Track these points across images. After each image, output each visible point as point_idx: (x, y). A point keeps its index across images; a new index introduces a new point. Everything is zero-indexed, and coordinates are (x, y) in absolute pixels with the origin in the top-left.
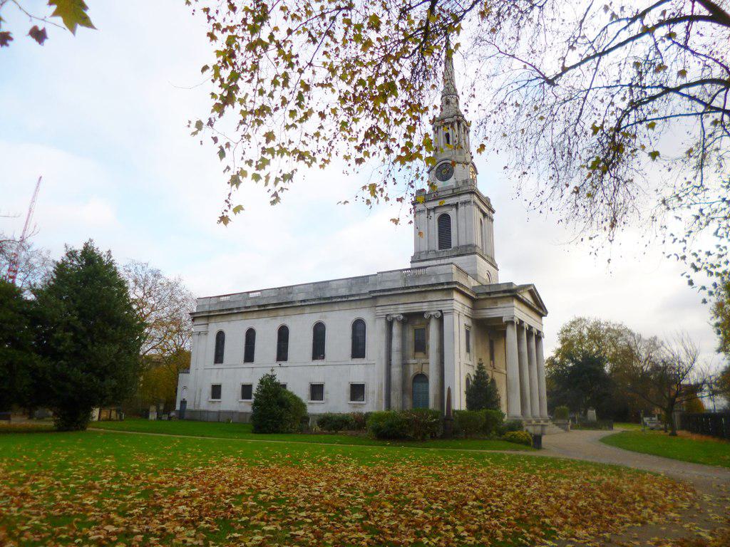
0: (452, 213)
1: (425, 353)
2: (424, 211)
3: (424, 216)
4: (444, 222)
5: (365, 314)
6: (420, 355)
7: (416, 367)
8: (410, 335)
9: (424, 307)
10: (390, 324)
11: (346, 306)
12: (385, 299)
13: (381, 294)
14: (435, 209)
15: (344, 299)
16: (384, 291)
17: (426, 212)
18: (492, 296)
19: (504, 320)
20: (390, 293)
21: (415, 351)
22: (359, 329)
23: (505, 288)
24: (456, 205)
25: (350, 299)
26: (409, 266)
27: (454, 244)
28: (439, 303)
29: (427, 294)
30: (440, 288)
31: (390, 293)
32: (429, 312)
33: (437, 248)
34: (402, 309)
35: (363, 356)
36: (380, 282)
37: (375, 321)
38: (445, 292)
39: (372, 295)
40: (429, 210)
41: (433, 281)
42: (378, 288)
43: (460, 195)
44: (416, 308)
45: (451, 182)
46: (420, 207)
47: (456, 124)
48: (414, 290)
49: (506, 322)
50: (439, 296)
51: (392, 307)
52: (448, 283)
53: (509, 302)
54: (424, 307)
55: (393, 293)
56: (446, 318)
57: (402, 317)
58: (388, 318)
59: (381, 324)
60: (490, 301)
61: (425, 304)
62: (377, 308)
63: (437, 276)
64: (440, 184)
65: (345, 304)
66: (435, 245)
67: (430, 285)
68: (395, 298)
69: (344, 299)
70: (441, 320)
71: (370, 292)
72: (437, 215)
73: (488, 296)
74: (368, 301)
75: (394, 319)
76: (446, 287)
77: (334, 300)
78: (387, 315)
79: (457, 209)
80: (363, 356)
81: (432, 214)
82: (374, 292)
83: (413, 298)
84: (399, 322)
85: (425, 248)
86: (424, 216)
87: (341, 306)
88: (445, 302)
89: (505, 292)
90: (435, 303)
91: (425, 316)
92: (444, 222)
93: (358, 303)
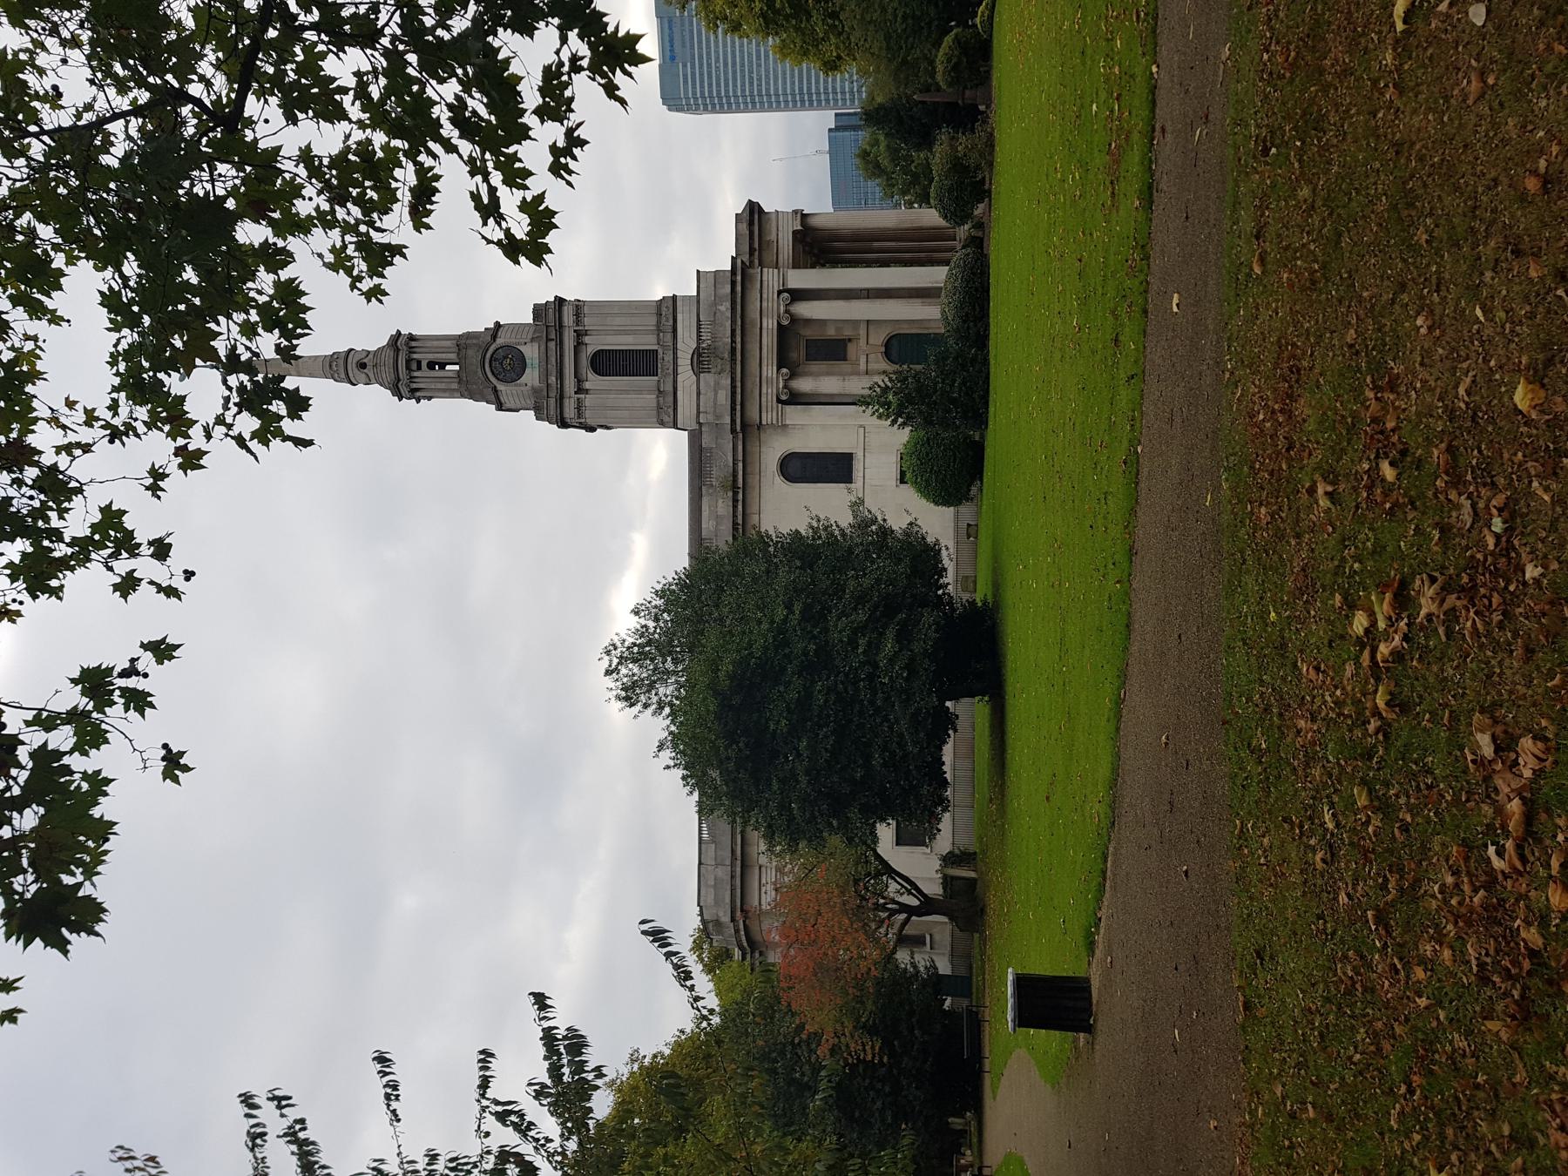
0: (593, 344)
1: (850, 340)
2: (578, 399)
3: (588, 400)
4: (607, 363)
5: (773, 451)
6: (851, 348)
7: (872, 357)
8: (815, 366)
9: (770, 326)
10: (795, 399)
11: (753, 495)
12: (748, 405)
13: (738, 407)
14: (579, 380)
15: (740, 496)
16: (733, 409)
17: (583, 396)
18: (756, 246)
19: (799, 228)
20: (739, 390)
21: (845, 359)
22: (802, 468)
23: (744, 226)
24: (579, 335)
25: (740, 483)
26: (683, 436)
27: (647, 342)
28: (765, 296)
29: (748, 321)
30: (739, 288)
31: (739, 390)
32: (779, 317)
33: (656, 378)
34: (770, 370)
35: (848, 458)
36: (718, 417)
37: (785, 426)
38: (748, 285)
39: (738, 428)
40: (580, 390)
41: (725, 307)
42: (728, 420)
43: (561, 326)
44: (769, 340)
45: (531, 352)
46: (570, 412)
47: (413, 344)
48: (738, 339)
49: (802, 225)
50: (754, 296)
51: (764, 390)
52: (733, 283)
53: (769, 219)
54: (770, 324)
55: (739, 384)
56: (792, 284)
57: (785, 370)
58: (784, 398)
59: (794, 414)
60: (765, 254)
61: (765, 325)
62: (764, 422)
63: (715, 304)
64: (531, 377)
65: (749, 497)
66: (650, 381)
67: (733, 309)
68: (749, 385)
69: (740, 496)
70: (798, 295)
71: (733, 431)
72: (591, 376)
73: (757, 253)
74: (749, 448)
75: (785, 387)
76: (739, 278)
77: (740, 521)
78: (779, 401)
79: (586, 333)
80: (848, 458)
81: (587, 385)
82: (733, 421)
83: (753, 348)
84: (790, 378)
85: (650, 399)
86: (588, 400)
87: (753, 508)
88: (765, 284)
89: (751, 223)
90: (765, 304)
91: (785, 323)
92: (607, 363)
93: (749, 469)
